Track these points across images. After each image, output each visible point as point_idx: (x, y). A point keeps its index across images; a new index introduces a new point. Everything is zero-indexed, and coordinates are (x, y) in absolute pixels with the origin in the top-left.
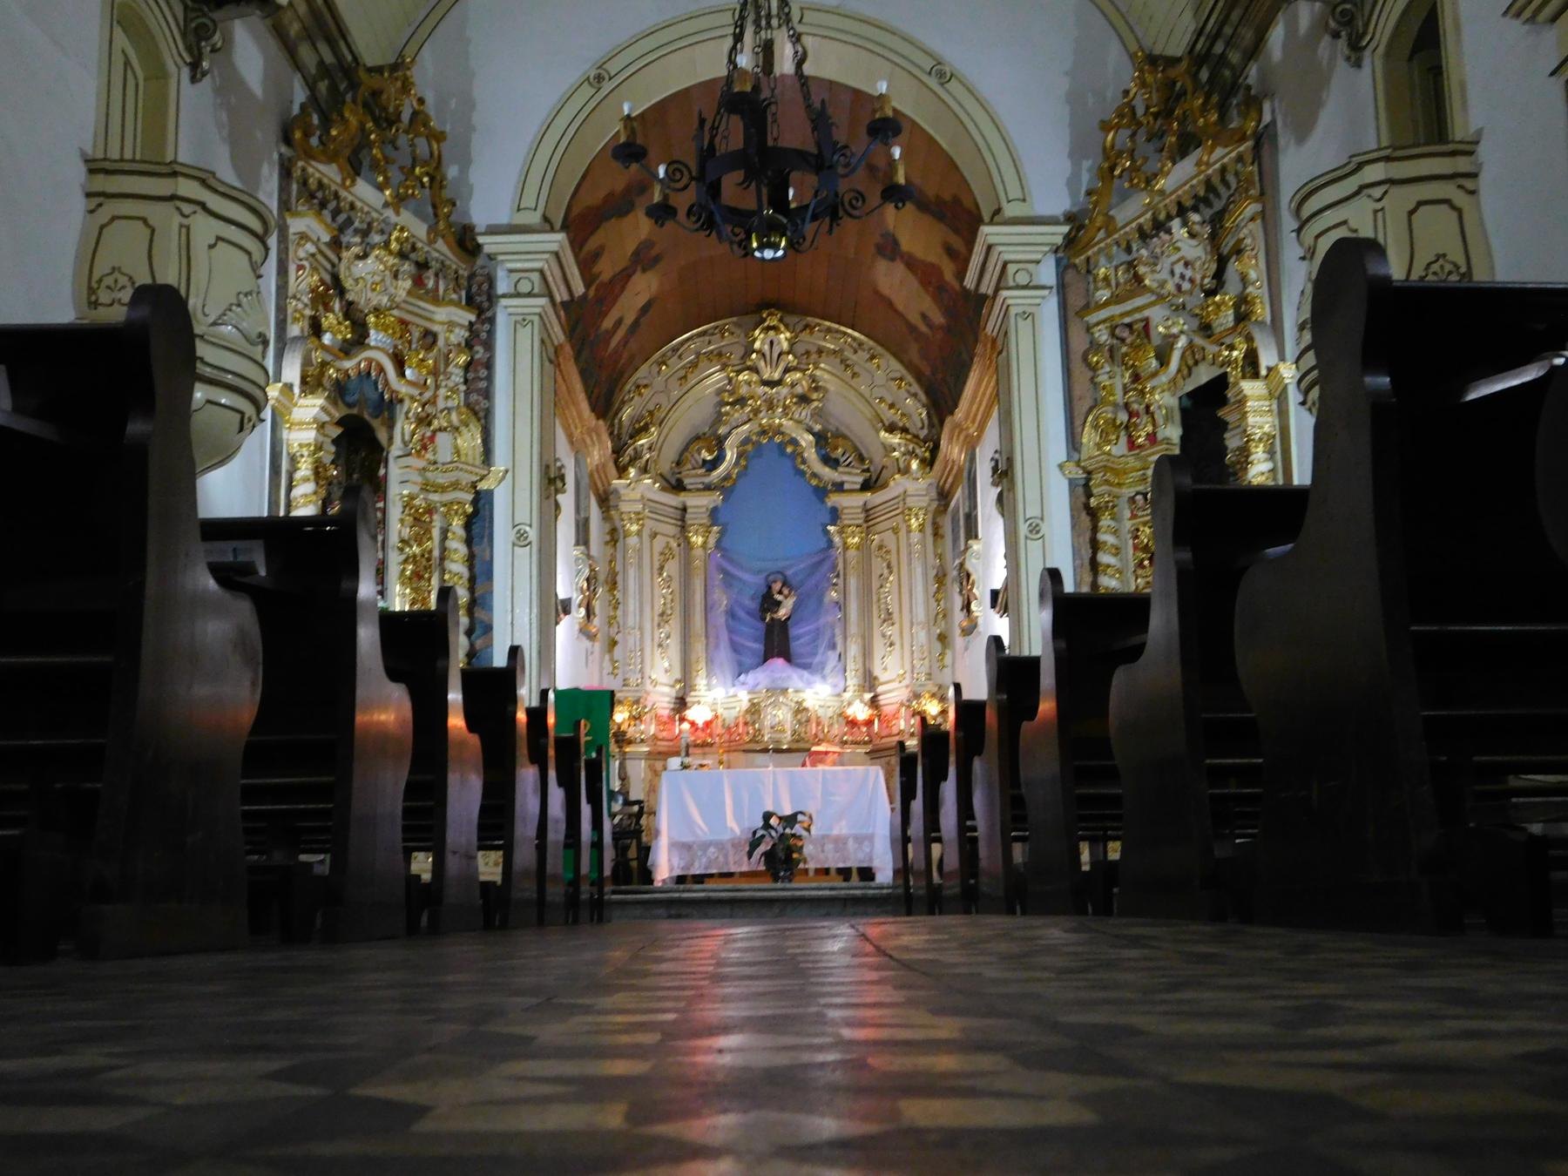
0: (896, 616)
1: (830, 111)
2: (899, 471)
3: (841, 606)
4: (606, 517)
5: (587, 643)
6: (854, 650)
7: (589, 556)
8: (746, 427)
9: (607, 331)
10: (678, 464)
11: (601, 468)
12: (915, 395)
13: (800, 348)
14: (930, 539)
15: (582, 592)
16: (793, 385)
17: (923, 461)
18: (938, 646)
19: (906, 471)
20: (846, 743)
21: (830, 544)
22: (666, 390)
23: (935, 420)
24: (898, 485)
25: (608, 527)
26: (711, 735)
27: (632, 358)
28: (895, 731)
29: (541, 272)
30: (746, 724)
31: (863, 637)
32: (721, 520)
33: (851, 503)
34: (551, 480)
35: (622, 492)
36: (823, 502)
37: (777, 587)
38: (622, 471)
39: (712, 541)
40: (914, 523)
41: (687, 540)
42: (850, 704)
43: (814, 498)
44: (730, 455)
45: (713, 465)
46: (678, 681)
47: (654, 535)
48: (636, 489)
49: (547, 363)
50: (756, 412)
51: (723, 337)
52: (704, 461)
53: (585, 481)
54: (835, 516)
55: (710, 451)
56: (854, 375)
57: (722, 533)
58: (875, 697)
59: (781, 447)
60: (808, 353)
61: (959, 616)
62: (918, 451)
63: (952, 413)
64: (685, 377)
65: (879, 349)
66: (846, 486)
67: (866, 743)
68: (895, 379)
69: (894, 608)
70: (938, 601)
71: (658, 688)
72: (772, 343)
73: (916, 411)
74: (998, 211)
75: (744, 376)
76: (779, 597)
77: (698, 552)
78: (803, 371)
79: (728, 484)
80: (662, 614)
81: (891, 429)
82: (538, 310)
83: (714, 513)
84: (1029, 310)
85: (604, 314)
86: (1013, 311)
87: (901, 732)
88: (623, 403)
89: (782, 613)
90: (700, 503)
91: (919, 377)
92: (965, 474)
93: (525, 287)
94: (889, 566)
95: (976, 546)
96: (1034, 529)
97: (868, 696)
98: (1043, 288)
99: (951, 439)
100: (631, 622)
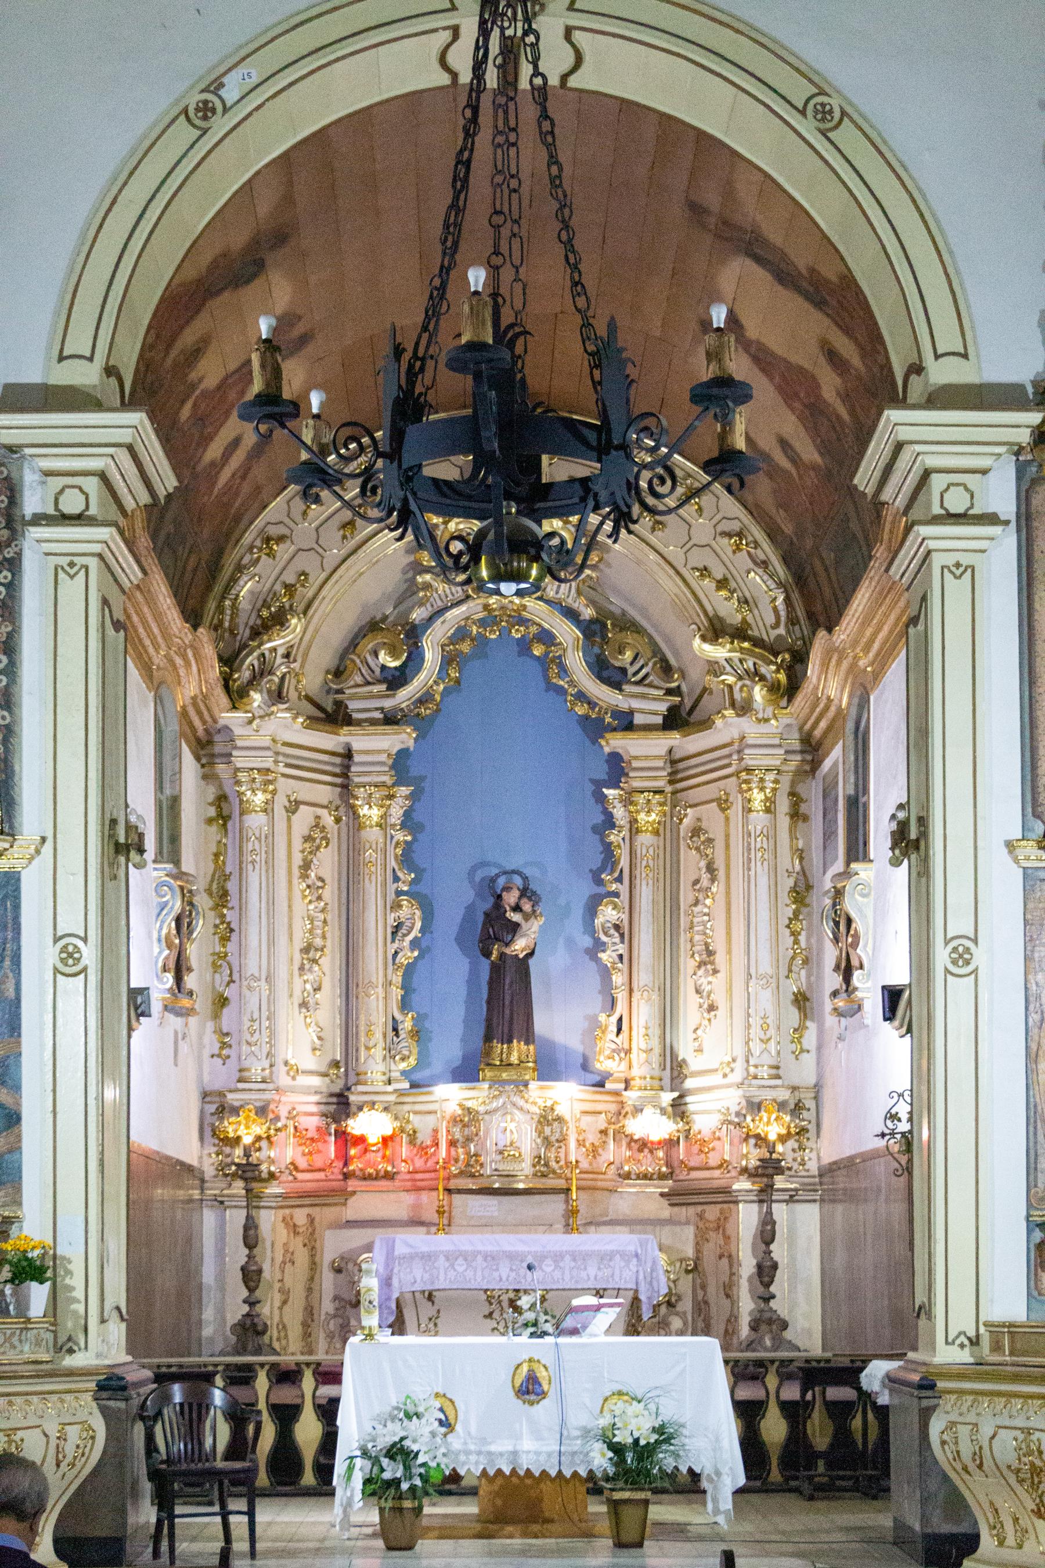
0: (720, 958)
1: (623, 339)
2: (733, 704)
3: (624, 932)
4: (208, 776)
5: (175, 1022)
6: (644, 1013)
7: (179, 875)
8: (463, 608)
9: (213, 464)
11: (202, 702)
12: (765, 564)
14: (784, 822)
15: (169, 945)
17: (773, 688)
18: (793, 1016)
19: (744, 708)
20: (627, 1176)
21: (610, 822)
22: (317, 548)
23: (800, 612)
24: (728, 727)
25: (211, 793)
26: (391, 1161)
27: (258, 489)
28: (713, 1160)
29: (103, 476)
30: (452, 1143)
31: (662, 990)
32: (414, 772)
33: (646, 749)
34: (121, 845)
35: (237, 731)
36: (594, 741)
37: (511, 898)
38: (236, 696)
39: (397, 813)
40: (758, 797)
41: (353, 810)
42: (638, 1110)
43: (578, 731)
44: (431, 656)
45: (396, 680)
46: (336, 1064)
47: (294, 806)
48: (268, 731)
49: (110, 631)
52: (383, 667)
53: (173, 727)
54: (617, 768)
55: (394, 653)
57: (413, 797)
58: (681, 1097)
59: (524, 647)
61: (833, 981)
63: (830, 630)
66: (639, 719)
67: (662, 1177)
69: (718, 944)
70: (795, 934)
71: (304, 1080)
73: (765, 597)
74: (916, 369)
76: (516, 917)
77: (372, 835)
80: (306, 950)
82: (97, 548)
83: (400, 762)
84: (965, 559)
85: (206, 440)
86: (938, 561)
87: (723, 1165)
88: (240, 568)
89: (519, 946)
90: (373, 745)
91: (773, 534)
92: (850, 725)
93: (72, 504)
94: (711, 869)
95: (863, 871)
96: (962, 957)
97: (667, 1097)
98: (991, 519)
99: (825, 666)
100: (252, 966)
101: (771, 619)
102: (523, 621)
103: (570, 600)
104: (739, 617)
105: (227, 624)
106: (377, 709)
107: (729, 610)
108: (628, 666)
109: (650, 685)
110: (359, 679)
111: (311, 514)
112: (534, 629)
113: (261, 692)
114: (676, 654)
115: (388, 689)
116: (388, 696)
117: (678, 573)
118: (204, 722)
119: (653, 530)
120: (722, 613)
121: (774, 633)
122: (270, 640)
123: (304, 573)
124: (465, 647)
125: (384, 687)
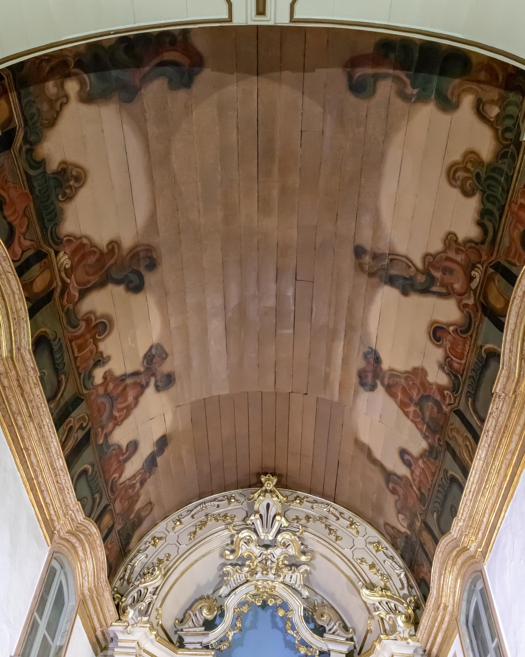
10: (181, 622)
13: (291, 515)
16: (286, 546)
35: (120, 637)
44: (229, 617)
50: (253, 572)
51: (230, 503)
56: (337, 538)
60: (297, 518)
62: (400, 608)
64: (195, 533)
65: (357, 519)
68: (371, 543)
72: (268, 506)
75: (245, 534)
78: (294, 533)
79: (224, 647)
81: (371, 587)
88: (139, 552)
101: (399, 586)
102: (275, 597)
103: (297, 586)
104: (382, 584)
105: (126, 577)
106: (199, 643)
107: (376, 579)
108: (326, 626)
109: (338, 635)
110: (190, 623)
111: (177, 528)
112: (279, 602)
113: (135, 611)
114: (350, 620)
115: (205, 630)
116: (204, 634)
117: (349, 561)
118: (101, 626)
119: (336, 540)
120: (373, 582)
121: (402, 593)
122: (145, 582)
123: (169, 555)
124: (245, 609)
125: (203, 628)
